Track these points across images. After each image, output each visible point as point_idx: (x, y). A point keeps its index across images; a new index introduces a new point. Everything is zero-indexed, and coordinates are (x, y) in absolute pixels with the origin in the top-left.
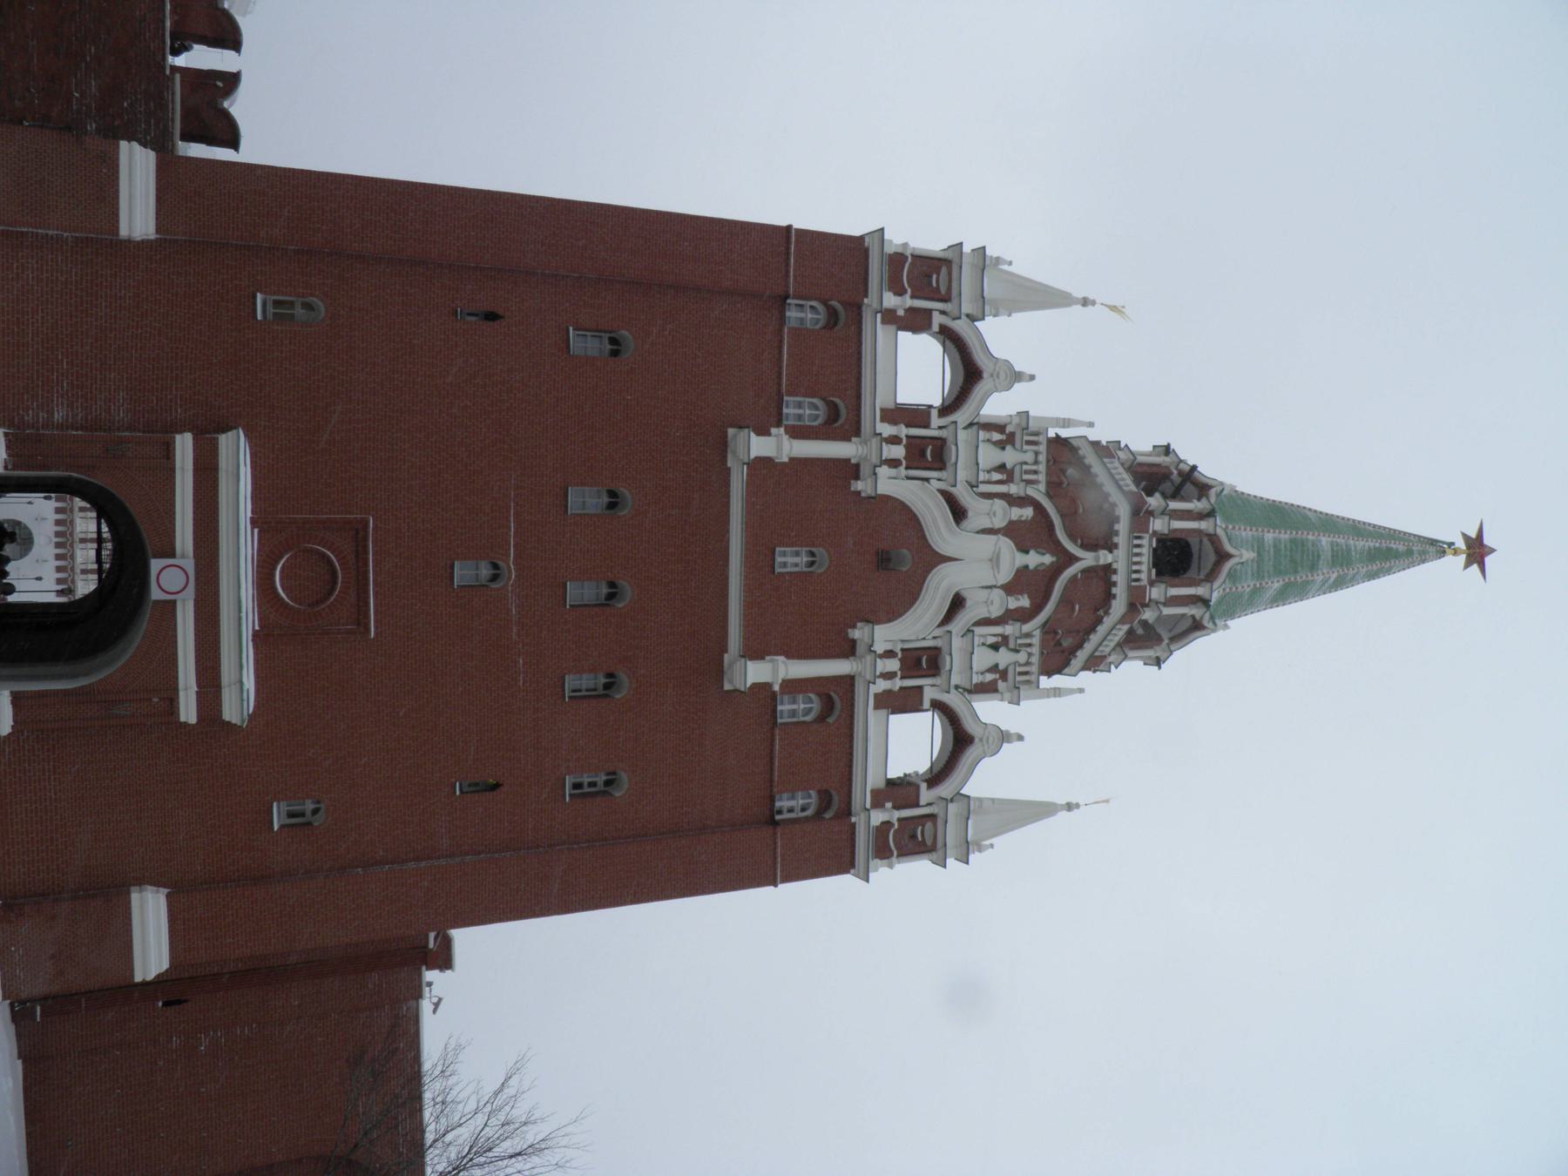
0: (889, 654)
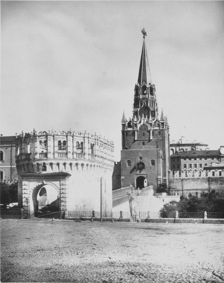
0: (150, 128)
